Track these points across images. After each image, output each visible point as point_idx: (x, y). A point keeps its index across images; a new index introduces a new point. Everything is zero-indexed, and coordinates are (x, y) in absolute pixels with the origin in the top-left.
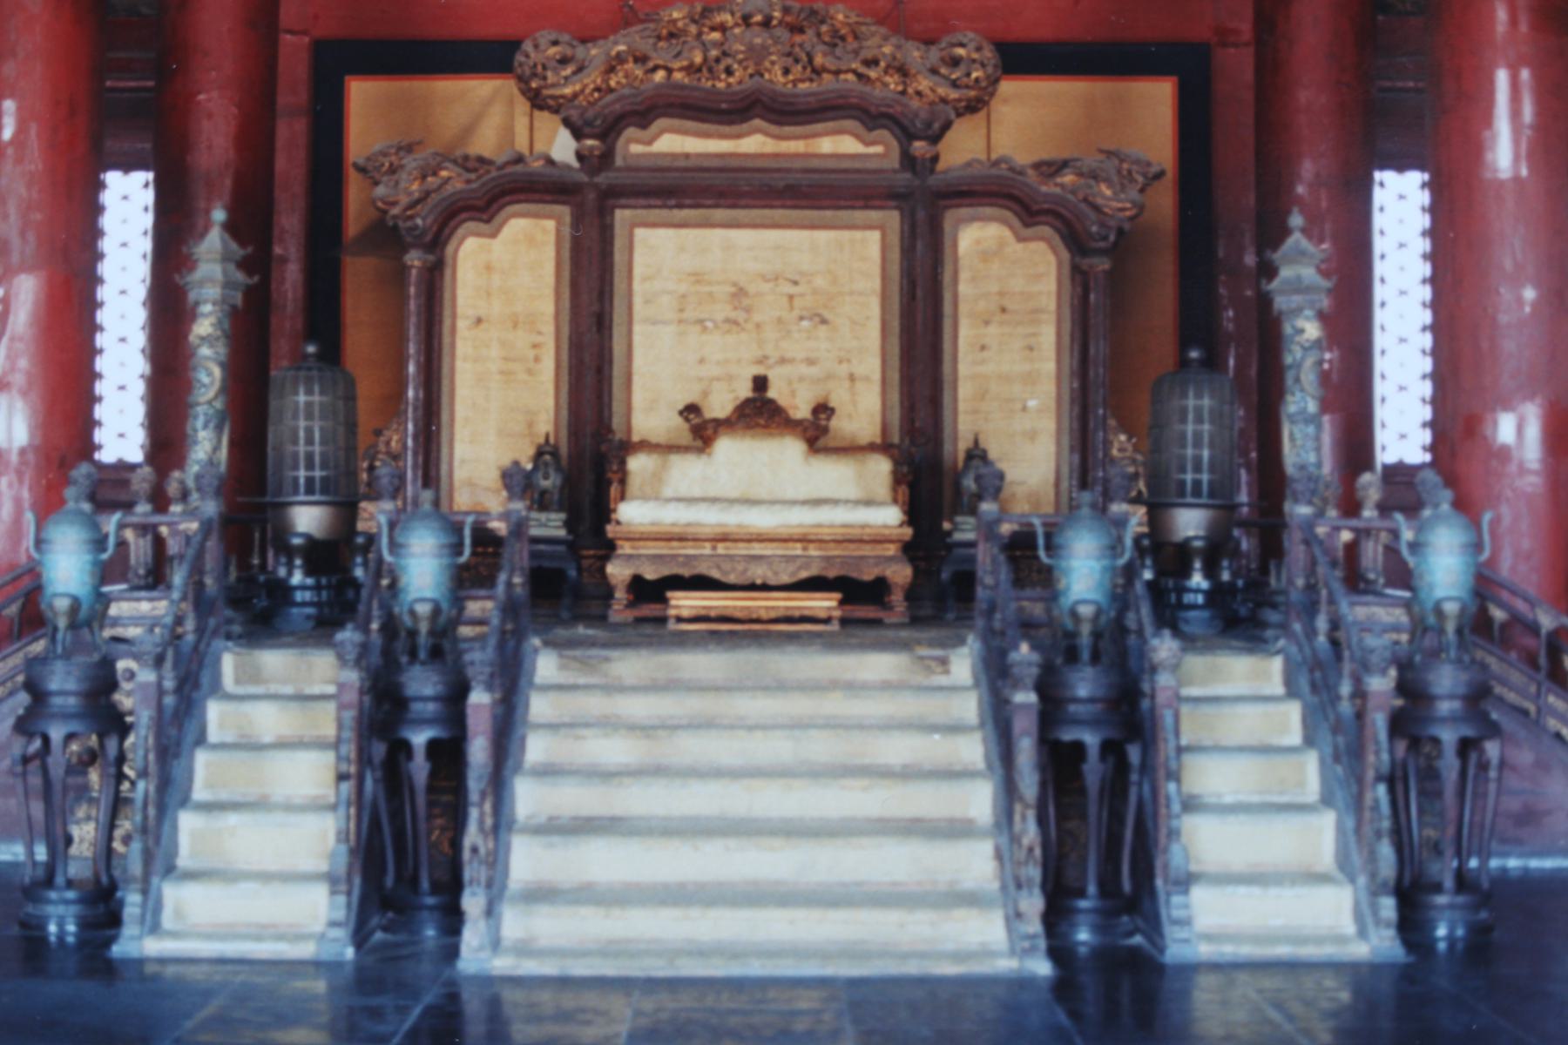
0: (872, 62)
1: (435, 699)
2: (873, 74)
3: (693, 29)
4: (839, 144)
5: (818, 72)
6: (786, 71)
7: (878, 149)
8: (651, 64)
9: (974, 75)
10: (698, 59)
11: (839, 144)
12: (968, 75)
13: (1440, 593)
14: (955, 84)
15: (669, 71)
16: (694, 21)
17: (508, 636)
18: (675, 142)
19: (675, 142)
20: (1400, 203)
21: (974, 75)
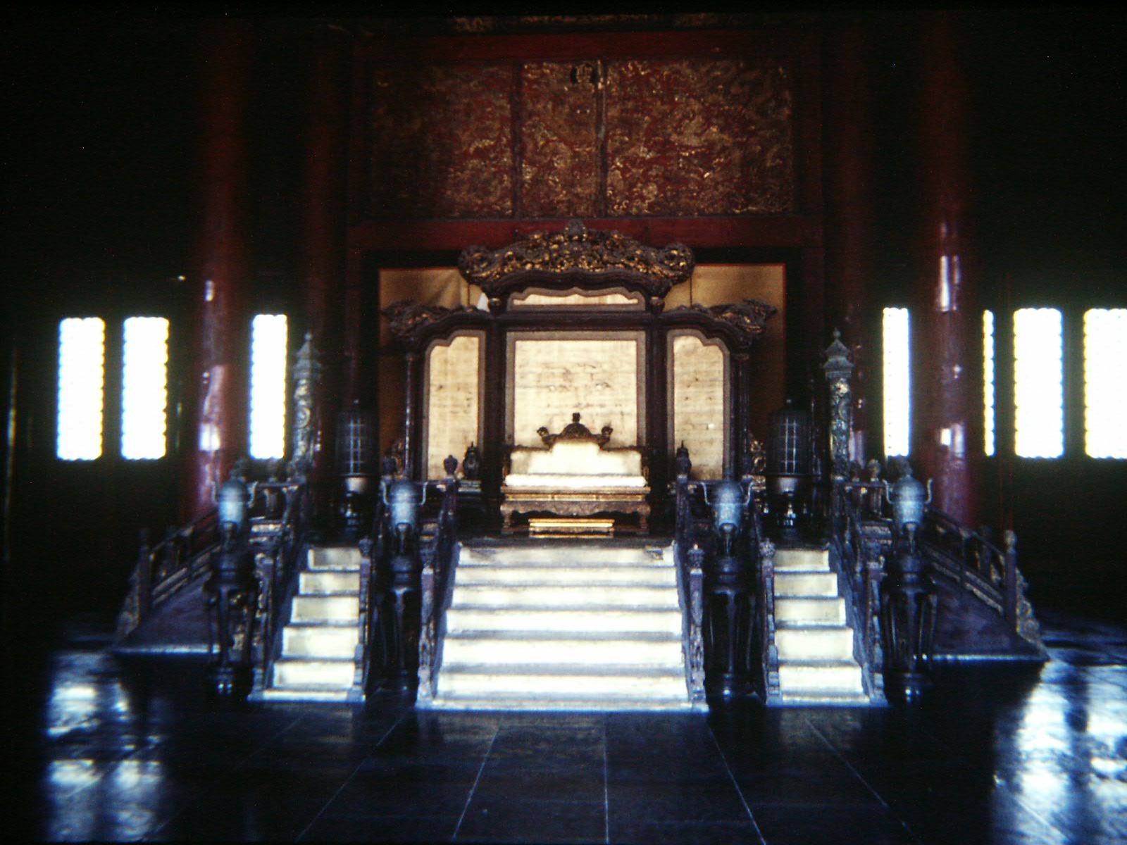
0: (631, 259)
1: (407, 572)
2: (632, 264)
3: (545, 244)
4: (616, 299)
5: (605, 263)
6: (589, 264)
7: (635, 301)
8: (524, 261)
9: (682, 264)
10: (547, 258)
11: (616, 299)
12: (679, 264)
13: (906, 520)
14: (671, 269)
15: (533, 264)
16: (544, 239)
17: (445, 541)
18: (536, 299)
19: (536, 299)
20: (896, 324)
21: (682, 264)
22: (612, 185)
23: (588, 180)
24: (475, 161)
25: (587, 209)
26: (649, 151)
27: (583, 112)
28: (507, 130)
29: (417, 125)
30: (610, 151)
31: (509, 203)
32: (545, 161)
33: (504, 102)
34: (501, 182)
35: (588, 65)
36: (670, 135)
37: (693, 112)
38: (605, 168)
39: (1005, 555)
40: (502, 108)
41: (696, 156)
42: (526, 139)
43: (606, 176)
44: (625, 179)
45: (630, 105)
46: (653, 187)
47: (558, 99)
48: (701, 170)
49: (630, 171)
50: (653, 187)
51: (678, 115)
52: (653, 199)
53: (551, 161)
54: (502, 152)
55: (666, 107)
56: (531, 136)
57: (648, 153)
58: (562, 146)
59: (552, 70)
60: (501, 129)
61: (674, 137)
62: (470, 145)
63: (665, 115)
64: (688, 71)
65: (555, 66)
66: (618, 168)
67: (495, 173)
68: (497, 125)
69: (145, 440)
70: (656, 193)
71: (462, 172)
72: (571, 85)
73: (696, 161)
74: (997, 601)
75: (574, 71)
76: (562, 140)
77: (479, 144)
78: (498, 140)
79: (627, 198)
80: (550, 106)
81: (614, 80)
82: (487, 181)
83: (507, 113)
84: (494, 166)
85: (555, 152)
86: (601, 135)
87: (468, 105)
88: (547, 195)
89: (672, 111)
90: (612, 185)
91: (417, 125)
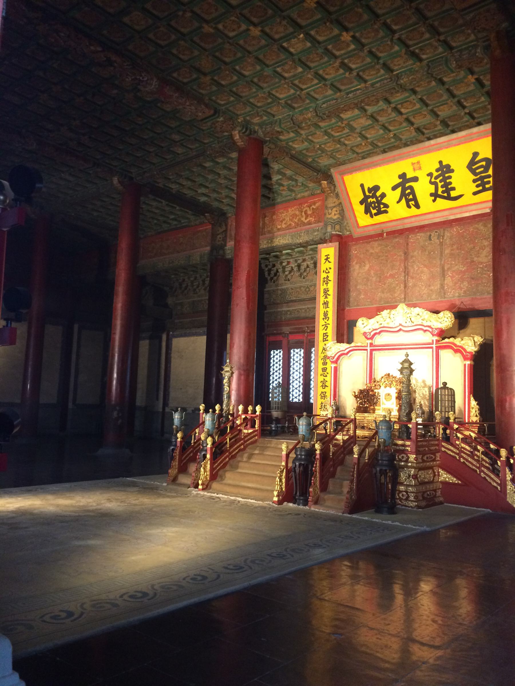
3: (388, 315)
22: (447, 284)
23: (436, 283)
24: (390, 280)
25: (436, 295)
26: (464, 267)
27: (434, 253)
28: (402, 265)
29: (367, 267)
30: (446, 268)
31: (403, 296)
32: (418, 277)
33: (402, 253)
34: (400, 287)
35: (436, 232)
36: (473, 258)
37: (484, 246)
38: (443, 275)
39: (500, 461)
40: (401, 256)
41: (486, 267)
42: (410, 268)
43: (444, 280)
44: (452, 281)
45: (455, 247)
46: (466, 283)
47: (423, 249)
48: (489, 273)
49: (455, 277)
50: (466, 283)
51: (477, 248)
52: (466, 288)
53: (421, 276)
54: (400, 274)
55: (472, 245)
56: (412, 266)
57: (463, 268)
58: (425, 269)
59: (421, 237)
60: (400, 265)
61: (475, 259)
62: (387, 273)
63: (471, 249)
64: (482, 228)
65: (422, 234)
66: (449, 276)
67: (397, 284)
68: (398, 263)
69: (296, 395)
70: (467, 285)
71: (384, 285)
72: (429, 242)
73: (486, 269)
74: (497, 483)
75: (430, 235)
76: (425, 266)
77: (390, 272)
78: (399, 269)
79: (453, 289)
80: (420, 252)
81: (448, 236)
82: (395, 287)
83: (403, 258)
84: (397, 281)
85: (422, 272)
86: (443, 262)
87: (387, 256)
88: (419, 291)
89: (474, 247)
90: (447, 284)
91: (367, 267)
